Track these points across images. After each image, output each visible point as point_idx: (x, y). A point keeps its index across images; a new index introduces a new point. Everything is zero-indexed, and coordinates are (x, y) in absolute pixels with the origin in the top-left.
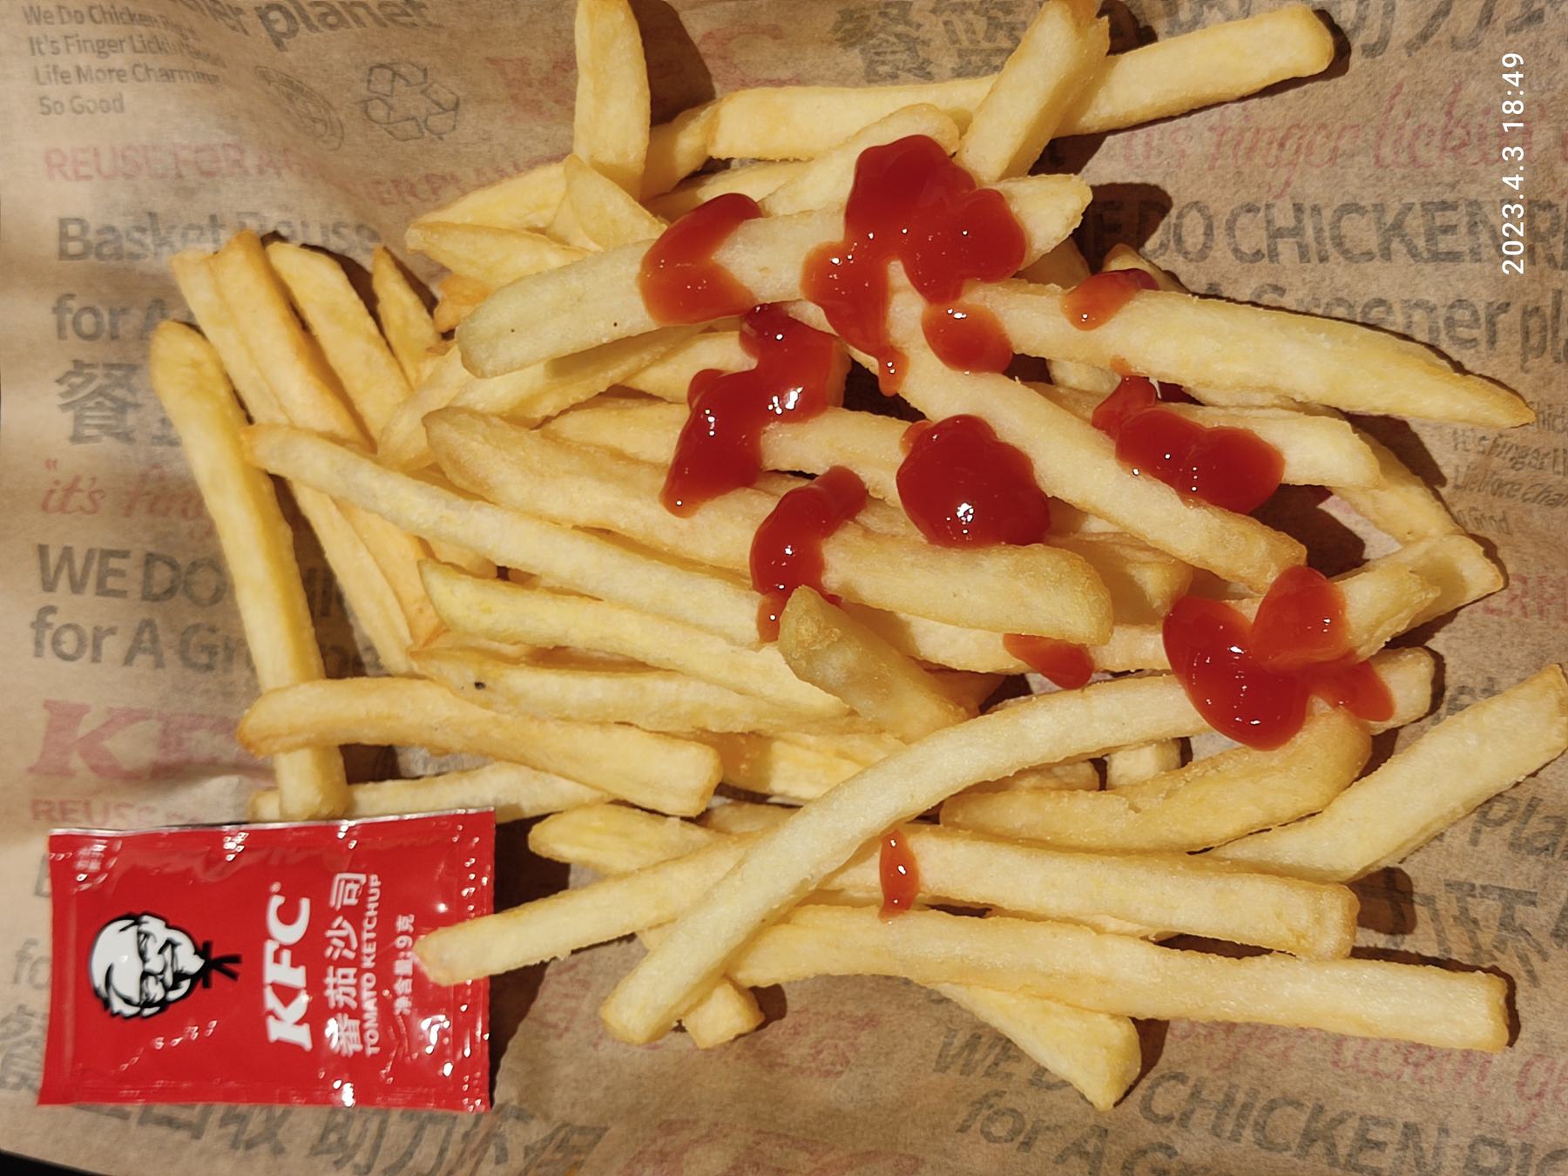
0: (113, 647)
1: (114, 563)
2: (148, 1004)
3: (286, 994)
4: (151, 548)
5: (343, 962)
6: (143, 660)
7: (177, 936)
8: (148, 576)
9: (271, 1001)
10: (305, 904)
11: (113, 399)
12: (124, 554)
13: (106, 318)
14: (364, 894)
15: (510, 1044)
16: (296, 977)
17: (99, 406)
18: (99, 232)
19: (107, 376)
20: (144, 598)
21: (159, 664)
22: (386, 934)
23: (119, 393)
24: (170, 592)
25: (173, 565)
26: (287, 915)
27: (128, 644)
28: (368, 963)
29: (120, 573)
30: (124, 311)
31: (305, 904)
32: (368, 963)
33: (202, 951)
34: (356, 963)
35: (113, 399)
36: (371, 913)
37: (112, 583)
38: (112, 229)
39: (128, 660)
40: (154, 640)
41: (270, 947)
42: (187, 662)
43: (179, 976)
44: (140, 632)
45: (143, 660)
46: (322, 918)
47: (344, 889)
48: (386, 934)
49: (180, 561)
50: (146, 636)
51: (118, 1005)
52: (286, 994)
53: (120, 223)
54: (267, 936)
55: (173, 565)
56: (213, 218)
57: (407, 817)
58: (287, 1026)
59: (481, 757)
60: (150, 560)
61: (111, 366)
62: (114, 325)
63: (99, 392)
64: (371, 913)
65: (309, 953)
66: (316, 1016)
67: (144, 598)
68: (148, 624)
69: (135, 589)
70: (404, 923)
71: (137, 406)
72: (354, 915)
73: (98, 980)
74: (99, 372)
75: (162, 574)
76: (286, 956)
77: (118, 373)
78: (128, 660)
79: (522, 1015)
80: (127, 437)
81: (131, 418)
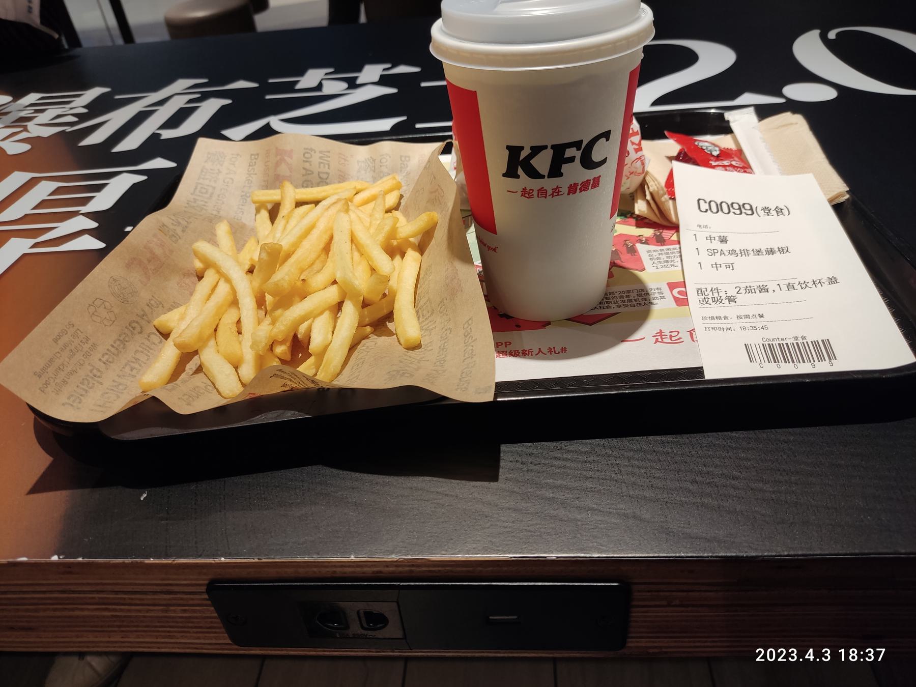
0: (307, 165)
1: (327, 166)
4: (330, 174)
6: (304, 172)
8: (324, 173)
11: (367, 168)
12: (329, 168)
13: (385, 164)
17: (366, 166)
18: (407, 164)
19: (373, 167)
20: (319, 172)
21: (303, 175)
23: (369, 169)
24: (320, 178)
25: (326, 179)
27: (307, 168)
29: (324, 167)
30: (387, 168)
35: (367, 168)
37: (322, 165)
38: (407, 167)
39: (304, 168)
40: (309, 174)
42: (303, 182)
44: (310, 171)
45: (304, 172)
49: (328, 180)
50: (310, 172)
53: (408, 169)
55: (326, 179)
56: (409, 185)
60: (327, 173)
61: (374, 167)
62: (383, 166)
63: (369, 165)
67: (319, 172)
68: (313, 173)
69: (320, 170)
71: (366, 173)
74: (373, 165)
75: (324, 176)
77: (373, 169)
78: (304, 168)
80: (359, 171)
81: (363, 172)
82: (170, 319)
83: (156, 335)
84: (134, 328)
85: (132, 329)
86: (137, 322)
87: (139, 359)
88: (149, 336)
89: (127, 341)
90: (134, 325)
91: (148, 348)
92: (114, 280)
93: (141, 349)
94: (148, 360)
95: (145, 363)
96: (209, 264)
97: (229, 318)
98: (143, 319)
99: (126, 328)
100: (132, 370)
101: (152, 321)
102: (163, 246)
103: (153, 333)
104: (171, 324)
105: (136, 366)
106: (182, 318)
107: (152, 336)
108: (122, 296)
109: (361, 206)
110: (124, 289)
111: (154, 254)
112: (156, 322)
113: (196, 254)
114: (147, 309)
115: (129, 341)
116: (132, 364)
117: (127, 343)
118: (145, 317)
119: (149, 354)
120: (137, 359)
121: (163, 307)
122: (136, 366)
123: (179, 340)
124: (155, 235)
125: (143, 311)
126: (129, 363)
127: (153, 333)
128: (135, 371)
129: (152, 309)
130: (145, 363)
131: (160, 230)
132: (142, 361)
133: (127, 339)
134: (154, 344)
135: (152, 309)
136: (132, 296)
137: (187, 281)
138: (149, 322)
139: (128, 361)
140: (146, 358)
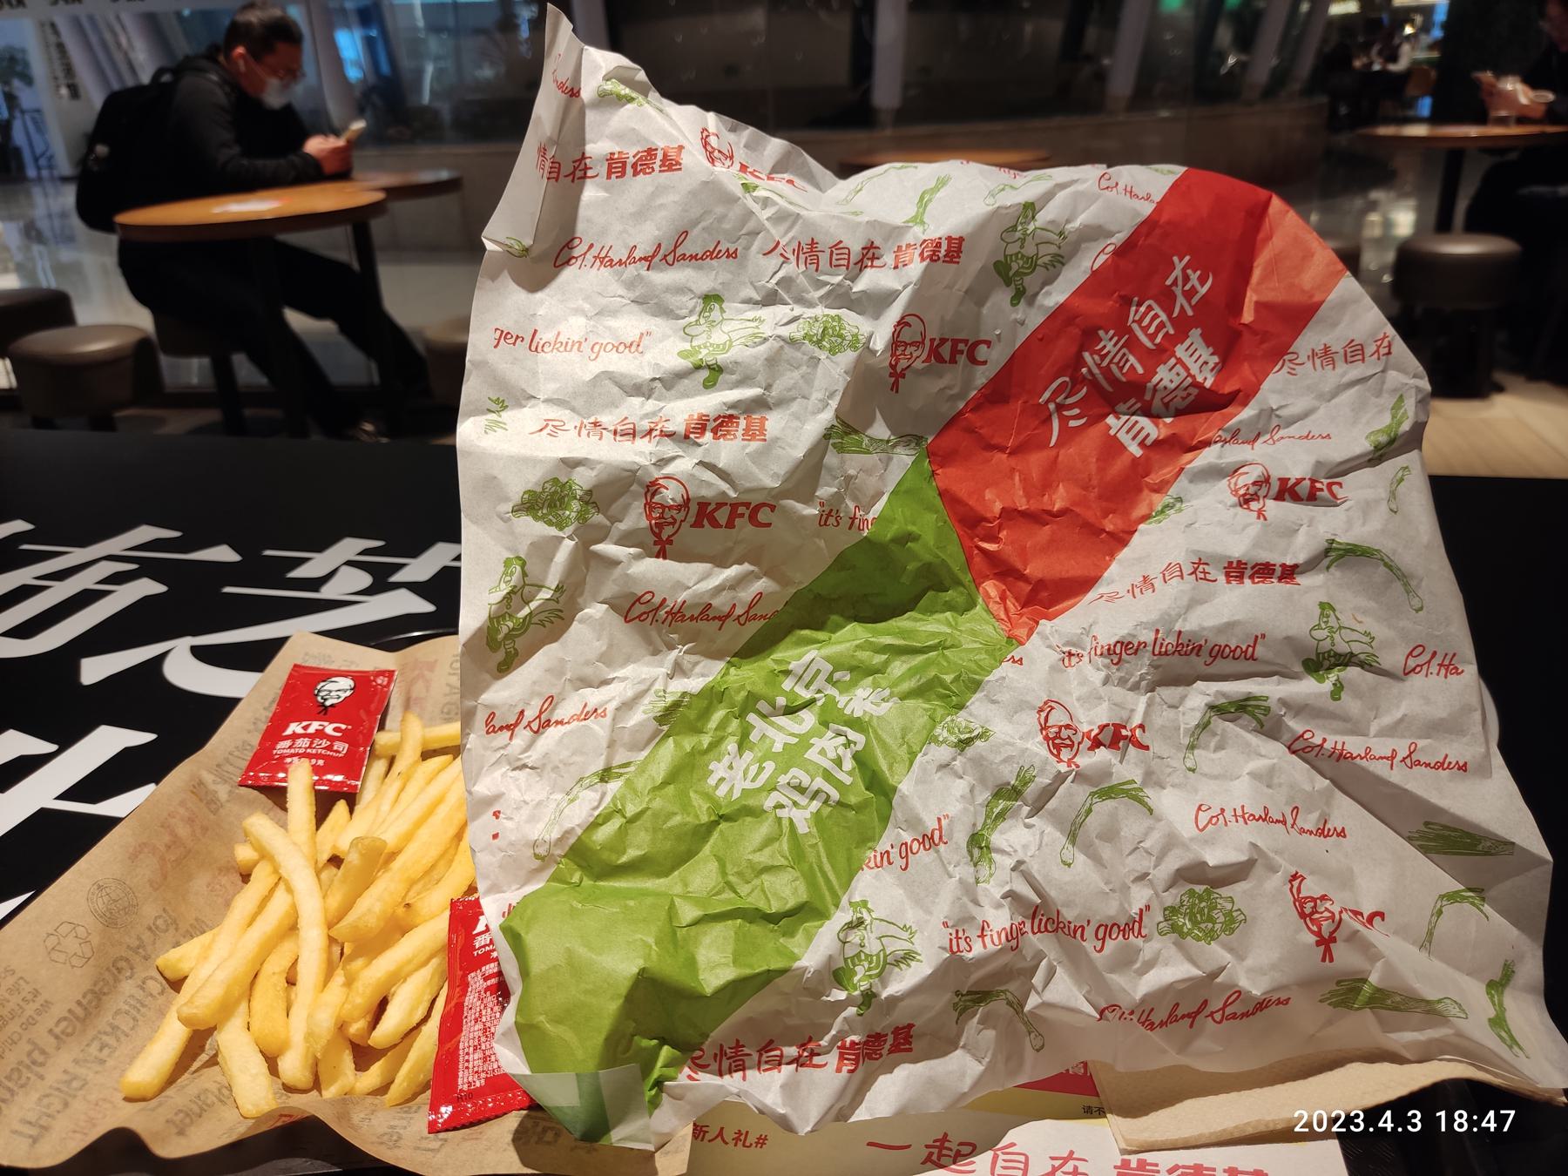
2: (319, 691)
3: (305, 728)
5: (312, 743)
7: (340, 700)
9: (304, 724)
10: (339, 734)
14: (337, 751)
15: (263, 796)
16: (311, 730)
22: (317, 756)
26: (336, 729)
28: (309, 750)
31: (339, 734)
32: (309, 750)
33: (332, 706)
34: (310, 747)
36: (328, 753)
41: (326, 724)
43: (325, 700)
46: (332, 739)
47: (342, 747)
48: (317, 756)
51: (322, 684)
52: (305, 728)
54: (331, 723)
57: (364, 768)
58: (295, 728)
59: (378, 792)
64: (328, 753)
65: (320, 734)
66: (295, 736)
70: (321, 762)
72: (329, 748)
73: (333, 679)
76: (321, 728)
79: (275, 803)
82: (181, 956)
83: (156, 980)
84: (120, 970)
85: (116, 972)
86: (127, 960)
87: (118, 1028)
88: (144, 983)
89: (105, 994)
90: (122, 964)
91: (138, 1005)
92: (99, 887)
93: (127, 1007)
94: (132, 1029)
95: (127, 1035)
96: (265, 855)
97: (276, 966)
98: (137, 953)
99: (108, 969)
100: (101, 1050)
101: (153, 956)
102: (193, 821)
103: (152, 978)
104: (185, 967)
105: (111, 1040)
106: (204, 957)
107: (150, 983)
108: (107, 914)
109: (374, 1028)
110: (115, 901)
111: (176, 835)
112: (160, 961)
113: (247, 837)
114: (146, 936)
115: (108, 993)
116: (105, 1038)
117: (104, 997)
118: (141, 950)
119: (138, 1017)
120: (115, 1028)
121: (177, 929)
122: (111, 1040)
123: (186, 1011)
124: (182, 803)
125: (139, 938)
126: (100, 1036)
127: (152, 978)
128: (106, 1051)
129: (155, 935)
130: (127, 1035)
131: (193, 792)
132: (123, 1032)
133: (105, 990)
134: (151, 995)
135: (155, 935)
136: (126, 914)
137: (224, 880)
138: (146, 958)
139: (99, 1032)
140: (131, 1023)
